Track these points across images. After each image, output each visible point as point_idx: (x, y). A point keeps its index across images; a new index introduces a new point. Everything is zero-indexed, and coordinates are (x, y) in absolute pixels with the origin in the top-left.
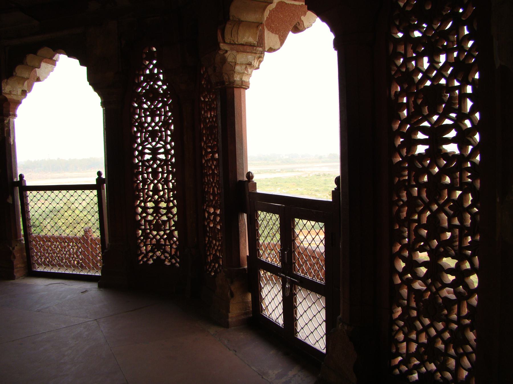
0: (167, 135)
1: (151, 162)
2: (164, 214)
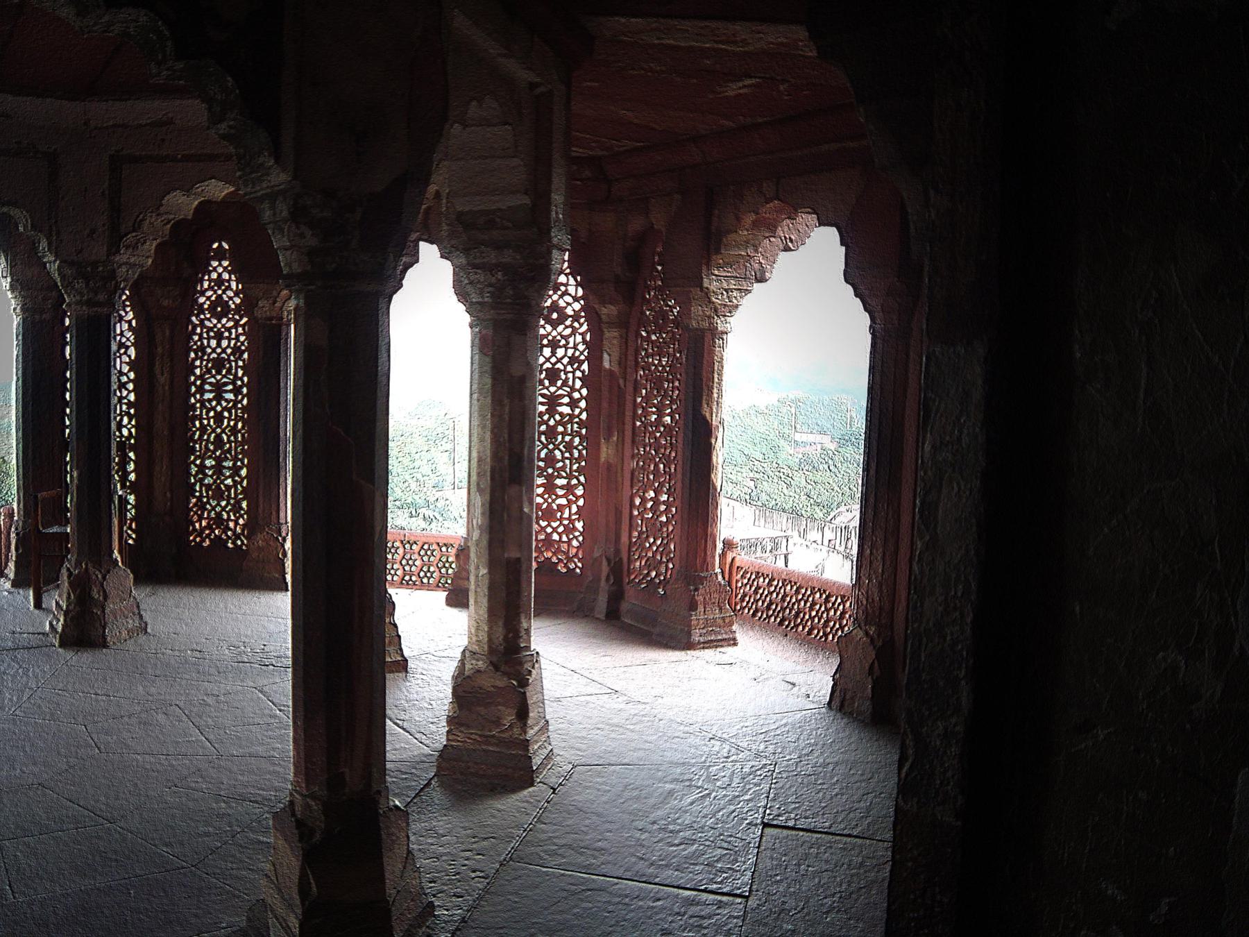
0: (237, 367)
1: (214, 403)
2: (229, 477)
